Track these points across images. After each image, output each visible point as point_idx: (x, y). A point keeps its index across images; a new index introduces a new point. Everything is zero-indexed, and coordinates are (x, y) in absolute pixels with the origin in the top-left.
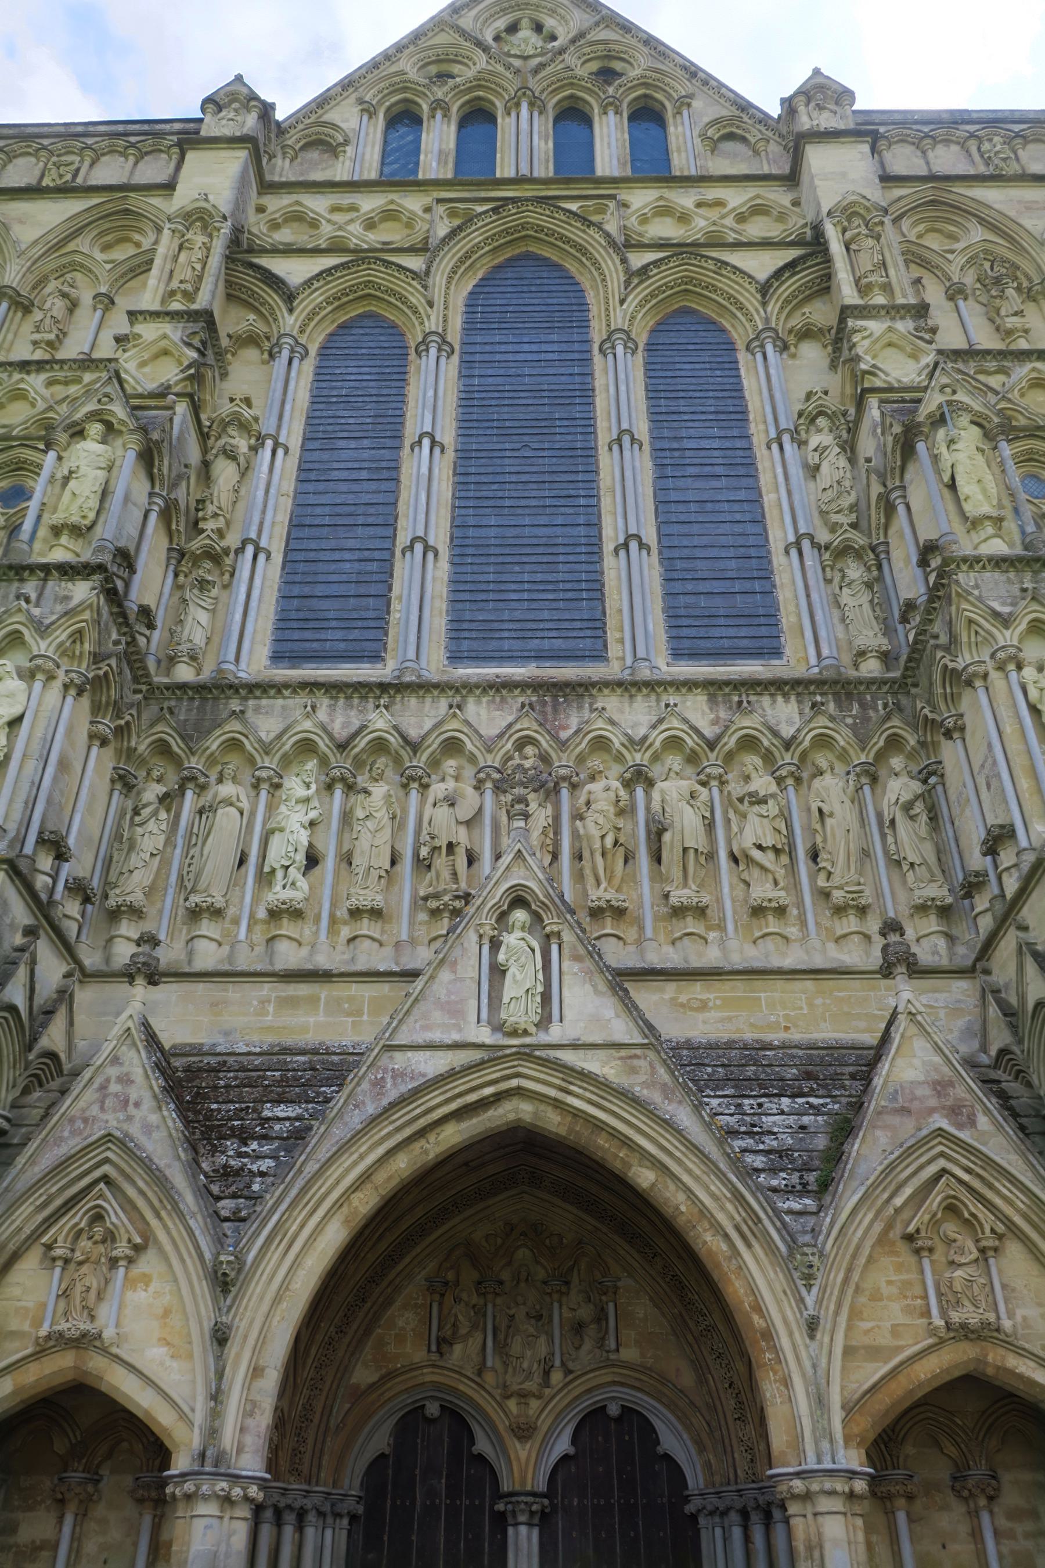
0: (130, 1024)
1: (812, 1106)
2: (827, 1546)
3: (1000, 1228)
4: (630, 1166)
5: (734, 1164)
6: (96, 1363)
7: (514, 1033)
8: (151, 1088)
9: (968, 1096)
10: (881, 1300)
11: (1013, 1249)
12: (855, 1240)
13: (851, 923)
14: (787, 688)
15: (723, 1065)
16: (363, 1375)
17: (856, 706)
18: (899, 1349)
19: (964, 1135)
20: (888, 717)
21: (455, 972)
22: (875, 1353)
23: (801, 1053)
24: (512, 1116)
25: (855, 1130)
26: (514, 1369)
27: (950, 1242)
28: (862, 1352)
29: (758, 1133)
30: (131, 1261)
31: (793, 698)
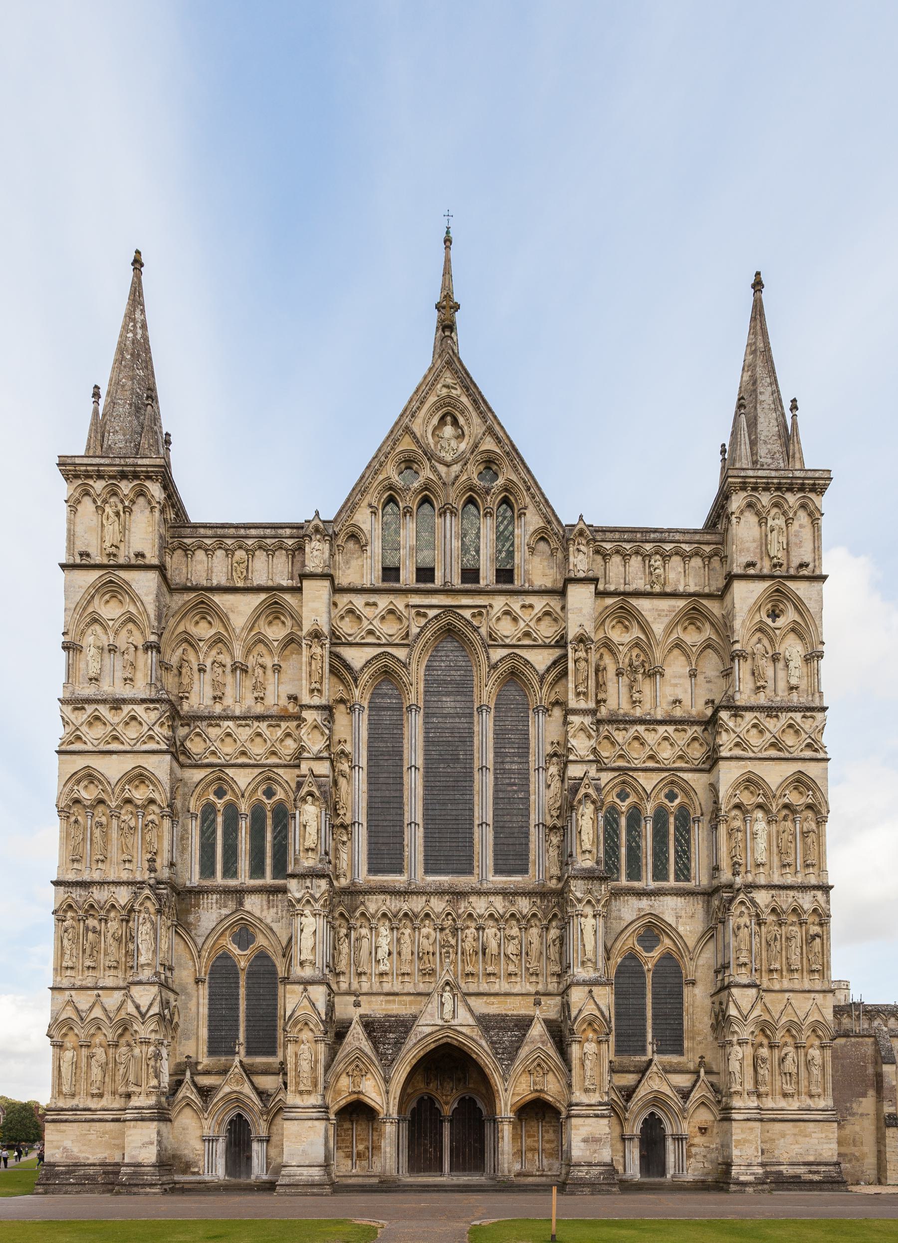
6: (362, 1097)
11: (551, 1074)
20: (554, 907)
22: (519, 1094)
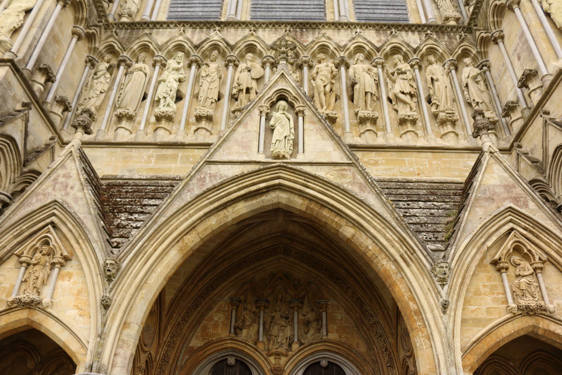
0: (72, 149)
1: (435, 205)
3: (545, 257)
4: (341, 226)
5: (400, 223)
7: (277, 157)
8: (80, 180)
9: (523, 193)
10: (480, 295)
12: (467, 262)
13: (449, 128)
14: (413, 28)
15: (387, 188)
16: (196, 343)
19: (523, 211)
20: (462, 41)
21: (246, 128)
22: (478, 322)
23: (427, 184)
24: (275, 201)
25: (466, 207)
26: (274, 341)
27: (516, 265)
28: (471, 321)
29: (408, 216)
30: (62, 265)
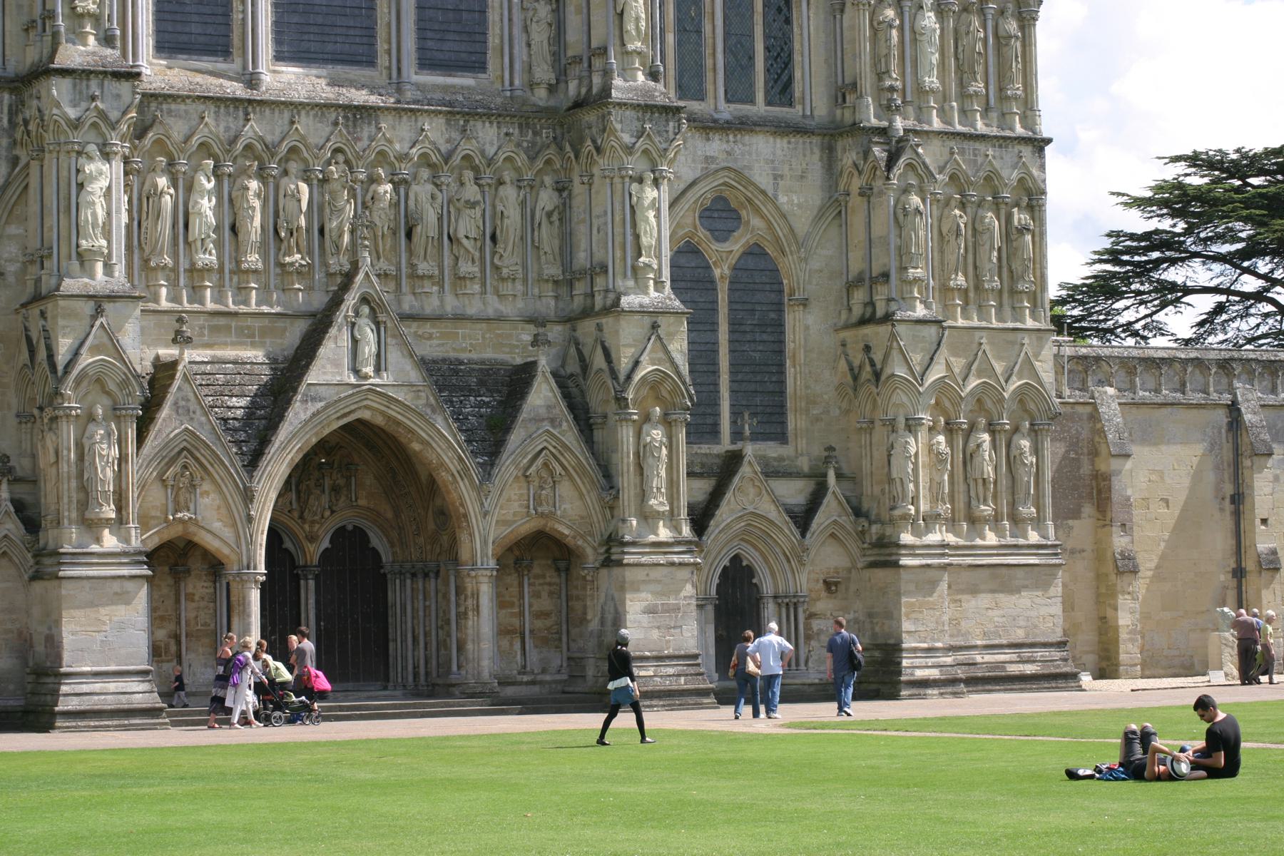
2: (481, 594)
3: (563, 473)
6: (192, 529)
17: (530, 132)
18: (515, 522)
27: (541, 478)
31: (495, 124)
